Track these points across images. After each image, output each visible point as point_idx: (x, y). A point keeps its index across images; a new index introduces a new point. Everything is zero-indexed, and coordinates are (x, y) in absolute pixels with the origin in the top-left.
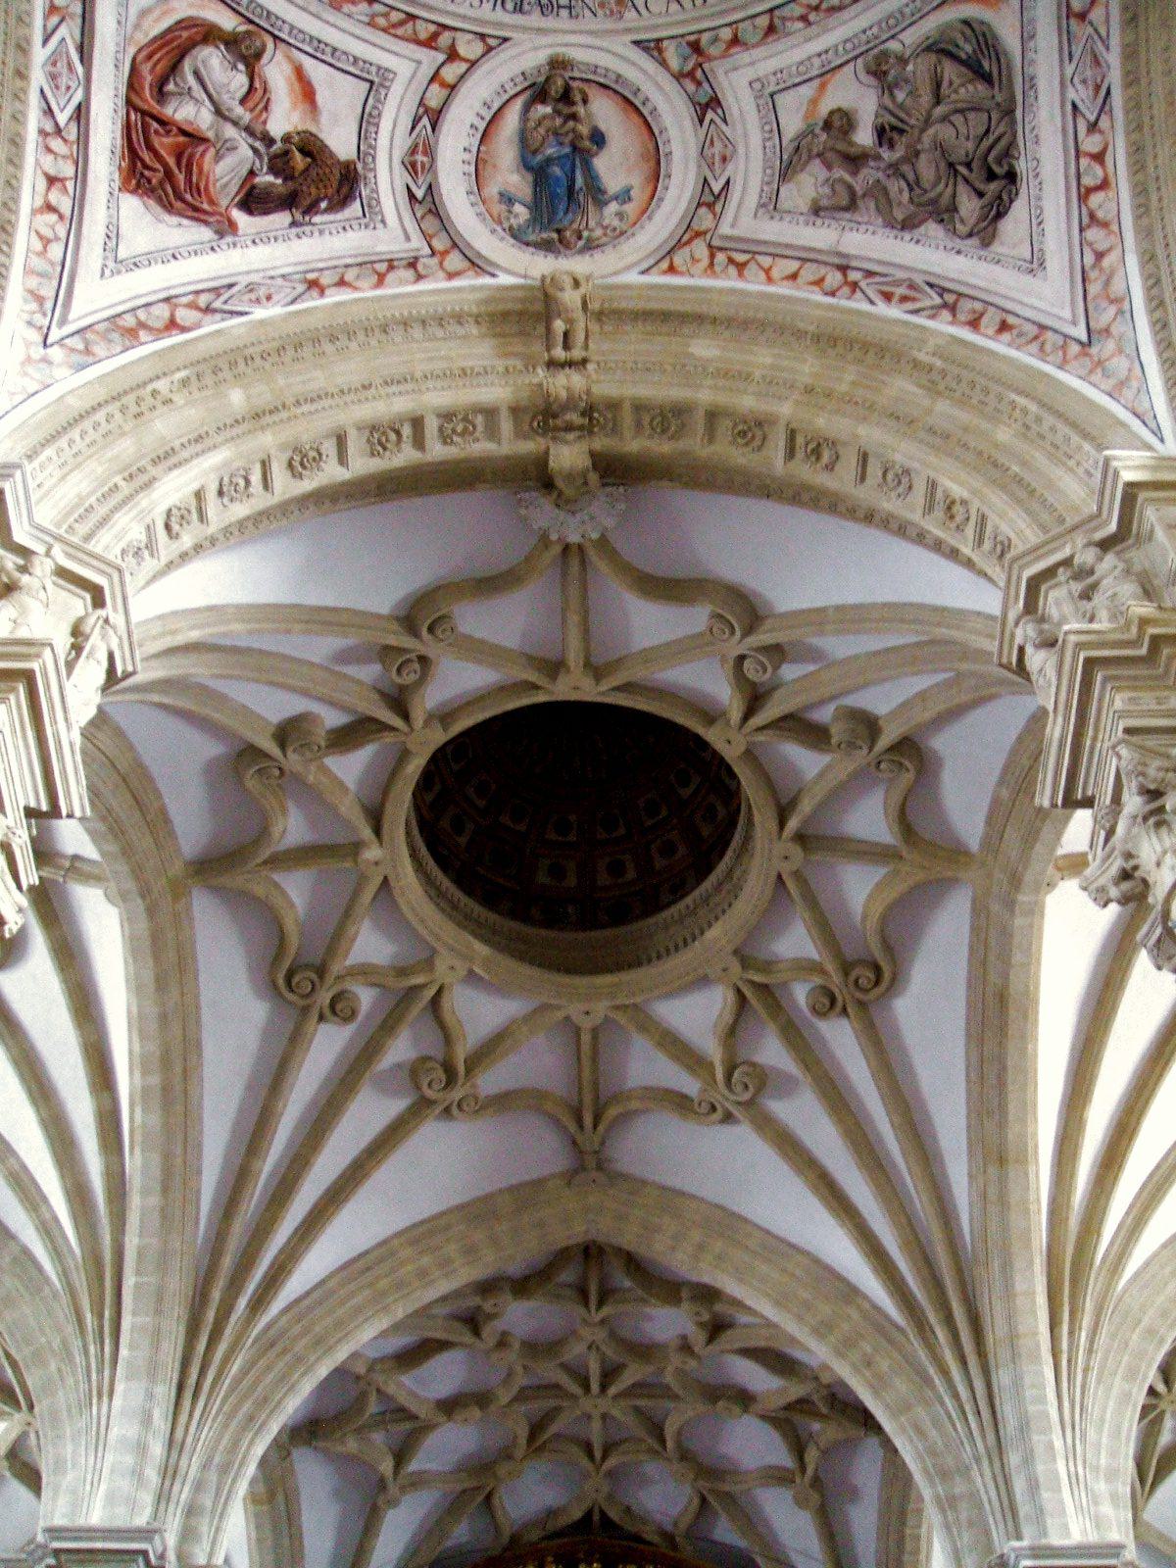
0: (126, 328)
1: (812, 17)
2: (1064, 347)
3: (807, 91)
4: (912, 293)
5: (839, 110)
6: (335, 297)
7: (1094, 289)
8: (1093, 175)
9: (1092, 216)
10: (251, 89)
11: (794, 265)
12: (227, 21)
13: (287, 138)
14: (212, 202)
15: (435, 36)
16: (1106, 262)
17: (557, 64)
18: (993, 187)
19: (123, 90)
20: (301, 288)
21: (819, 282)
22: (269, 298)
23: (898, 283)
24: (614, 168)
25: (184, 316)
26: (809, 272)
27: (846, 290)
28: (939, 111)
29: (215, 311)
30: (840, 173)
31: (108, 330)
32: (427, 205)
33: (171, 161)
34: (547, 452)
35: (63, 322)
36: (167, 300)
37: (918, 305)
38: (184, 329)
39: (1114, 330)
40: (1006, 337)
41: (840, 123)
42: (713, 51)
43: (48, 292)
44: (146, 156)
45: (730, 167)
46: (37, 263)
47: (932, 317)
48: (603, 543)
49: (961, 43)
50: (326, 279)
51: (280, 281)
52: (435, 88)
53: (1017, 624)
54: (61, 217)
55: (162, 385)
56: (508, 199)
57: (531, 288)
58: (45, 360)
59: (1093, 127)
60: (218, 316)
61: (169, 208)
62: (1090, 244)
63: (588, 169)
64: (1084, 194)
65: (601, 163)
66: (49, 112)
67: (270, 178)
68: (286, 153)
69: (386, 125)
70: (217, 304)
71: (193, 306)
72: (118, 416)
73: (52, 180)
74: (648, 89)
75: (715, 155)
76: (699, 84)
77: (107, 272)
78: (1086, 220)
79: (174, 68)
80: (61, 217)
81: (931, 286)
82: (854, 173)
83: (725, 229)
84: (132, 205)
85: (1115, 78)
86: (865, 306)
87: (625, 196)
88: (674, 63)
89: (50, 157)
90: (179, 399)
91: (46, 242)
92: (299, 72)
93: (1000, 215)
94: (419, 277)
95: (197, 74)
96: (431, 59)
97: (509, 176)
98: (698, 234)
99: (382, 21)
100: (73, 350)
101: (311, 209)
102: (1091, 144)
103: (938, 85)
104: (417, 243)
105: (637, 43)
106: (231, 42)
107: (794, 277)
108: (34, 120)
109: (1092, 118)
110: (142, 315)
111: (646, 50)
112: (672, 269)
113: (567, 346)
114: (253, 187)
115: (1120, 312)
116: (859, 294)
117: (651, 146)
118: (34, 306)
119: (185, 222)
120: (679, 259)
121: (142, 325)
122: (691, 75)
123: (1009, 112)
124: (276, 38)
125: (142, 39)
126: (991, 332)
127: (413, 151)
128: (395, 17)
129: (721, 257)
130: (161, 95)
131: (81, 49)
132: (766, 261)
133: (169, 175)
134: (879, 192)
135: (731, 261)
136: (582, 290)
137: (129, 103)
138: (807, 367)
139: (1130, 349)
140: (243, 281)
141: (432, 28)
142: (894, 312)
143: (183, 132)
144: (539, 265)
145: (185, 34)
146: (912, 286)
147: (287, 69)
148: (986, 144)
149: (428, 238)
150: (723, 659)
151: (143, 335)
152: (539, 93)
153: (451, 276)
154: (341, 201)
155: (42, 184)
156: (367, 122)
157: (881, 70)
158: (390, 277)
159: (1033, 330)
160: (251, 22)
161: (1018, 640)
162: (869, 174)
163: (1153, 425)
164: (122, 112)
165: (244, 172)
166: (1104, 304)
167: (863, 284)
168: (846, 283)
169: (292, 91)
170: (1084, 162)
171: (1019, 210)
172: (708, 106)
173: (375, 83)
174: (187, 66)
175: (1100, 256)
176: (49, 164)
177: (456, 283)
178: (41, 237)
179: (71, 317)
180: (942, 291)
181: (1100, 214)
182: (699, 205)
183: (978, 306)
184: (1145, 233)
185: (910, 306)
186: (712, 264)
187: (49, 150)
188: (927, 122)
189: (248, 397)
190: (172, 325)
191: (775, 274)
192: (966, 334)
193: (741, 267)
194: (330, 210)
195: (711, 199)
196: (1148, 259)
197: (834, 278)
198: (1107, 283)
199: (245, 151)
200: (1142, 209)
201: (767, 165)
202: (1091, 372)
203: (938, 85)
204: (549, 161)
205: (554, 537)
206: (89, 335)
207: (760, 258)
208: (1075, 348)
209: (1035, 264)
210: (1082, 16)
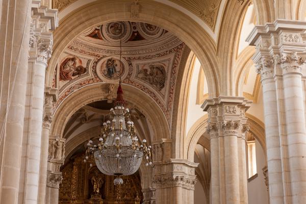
0: (61, 99)
12: (71, 57)
24: (118, 69)
30: (145, 76)
41: (146, 71)
56: (104, 71)
64: (170, 93)
65: (116, 68)
75: (131, 70)
79: (66, 64)
84: (61, 81)
85: (175, 83)
92: (80, 60)
97: (105, 68)
103: (157, 73)
104: (94, 77)
107: (138, 86)
123: (164, 79)
127: (93, 66)
134: (149, 79)
138: (138, 98)
142: (149, 95)
154: (84, 72)
156: (88, 64)
157: (152, 67)
162: (148, 77)
171: (164, 88)
172: (130, 64)
173: (89, 61)
175: (170, 101)
190: (66, 95)
197: (143, 87)
199: (73, 70)
203: (157, 73)
209: (163, 97)
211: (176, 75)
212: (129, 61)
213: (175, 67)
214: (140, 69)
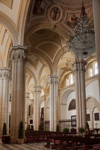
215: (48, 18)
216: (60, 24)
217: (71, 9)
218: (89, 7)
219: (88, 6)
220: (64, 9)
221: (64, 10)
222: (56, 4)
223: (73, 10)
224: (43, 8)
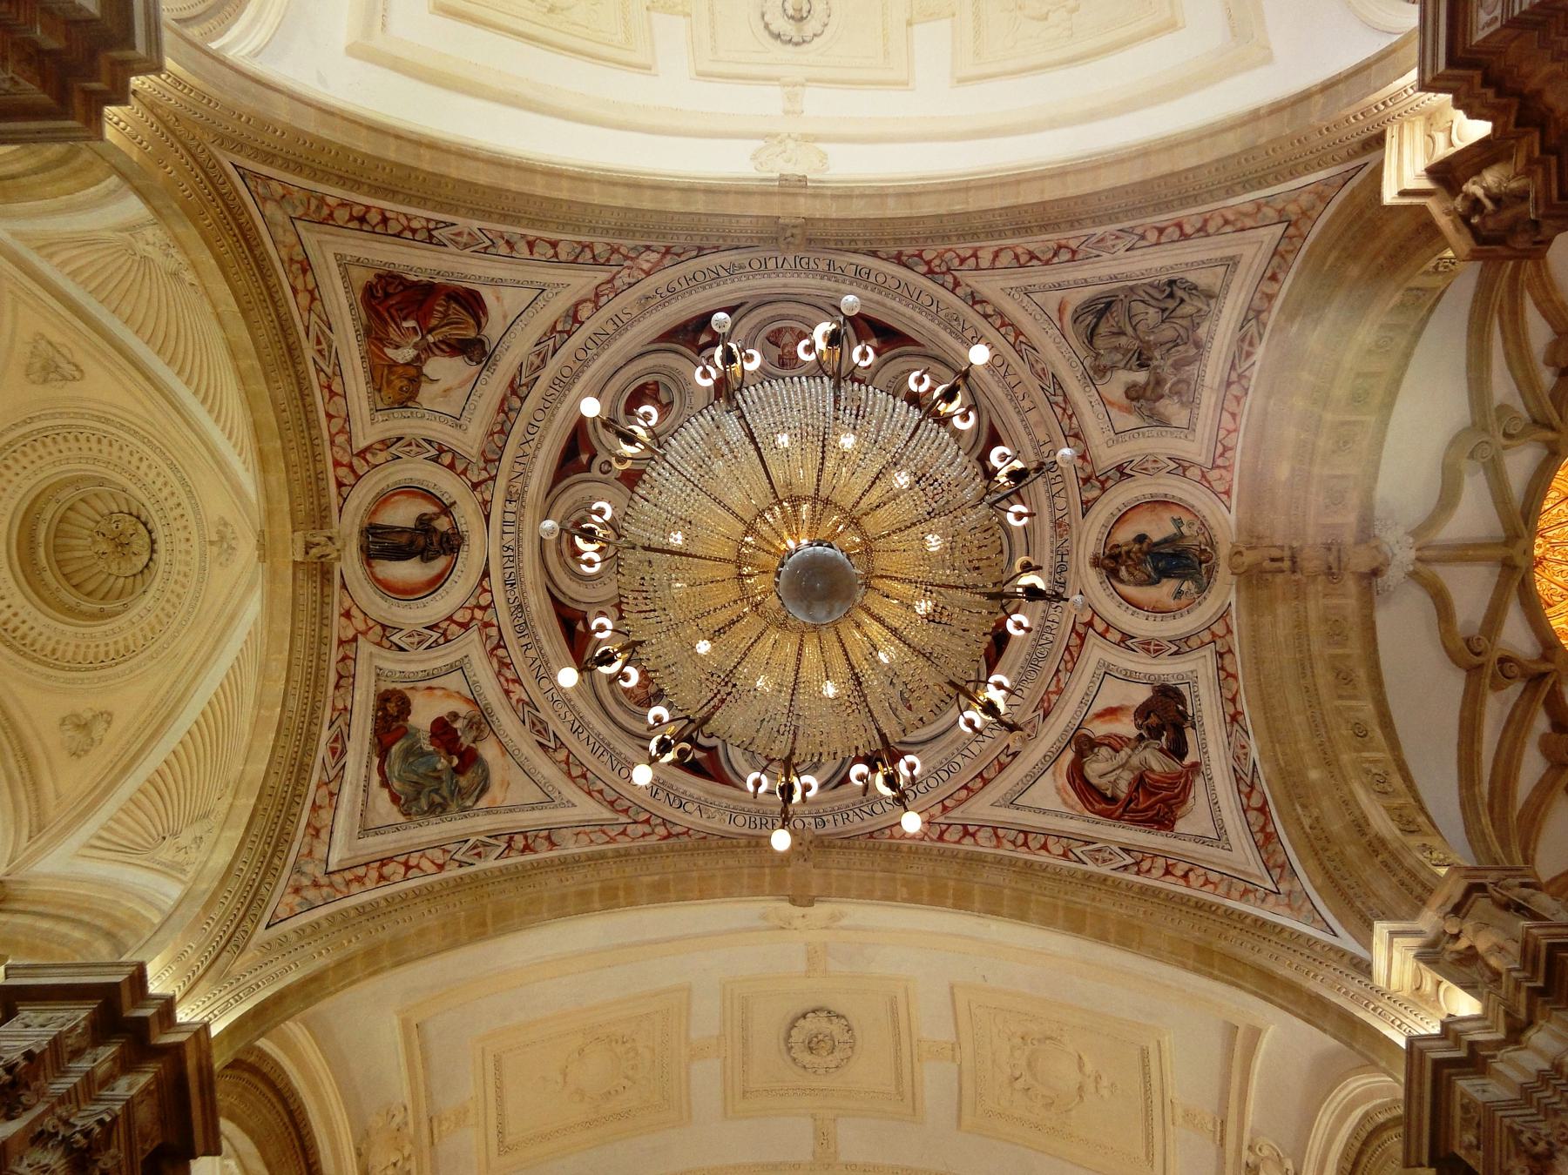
0: (1265, 840)
1: (1070, 412)
2: (1291, 238)
3: (1114, 413)
4: (1248, 337)
5: (1126, 393)
6: (1243, 705)
7: (1249, 222)
8: (1173, 232)
9: (1199, 230)
10: (1109, 745)
11: (1226, 416)
12: (1069, 755)
13: (1139, 727)
14: (1180, 777)
15: (1078, 634)
16: (1231, 217)
17: (1096, 563)
18: (1179, 293)
19: (1110, 821)
20: (1236, 726)
21: (1238, 399)
22: (1243, 747)
23: (1240, 349)
24: (1158, 528)
25: (1256, 801)
26: (1231, 405)
27: (1244, 382)
28: (1129, 330)
29: (1252, 782)
31: (1266, 852)
32: (1181, 647)
33: (1153, 799)
34: (1353, 573)
35: (1262, 879)
36: (1245, 811)
37: (1256, 335)
38: (1266, 802)
39: (1280, 207)
40: (1281, 276)
41: (1134, 394)
42: (1089, 470)
43: (1242, 886)
44: (1151, 813)
45: (1160, 457)
46: (1222, 889)
47: (1265, 325)
48: (1415, 533)
49: (1087, 322)
50: (1232, 711)
51: (1232, 739)
52: (1109, 636)
53: (1515, 249)
54: (1191, 870)
55: (1307, 822)
56: (1179, 594)
57: (1238, 582)
58: (1289, 894)
59: (1143, 237)
60: (1256, 780)
61: (1184, 802)
62: (1219, 229)
63: (1157, 544)
65: (1156, 536)
66: (1126, 868)
67: (1163, 739)
68: (1148, 728)
69: (1131, 666)
70: (1248, 781)
71: (1249, 796)
72: (1327, 854)
73: (1167, 872)
74: (1112, 508)
76: (1108, 478)
77: (1227, 847)
78: (1202, 234)
80: (1191, 870)
81: (1242, 327)
82: (1165, 381)
83: (1200, 460)
84: (1180, 826)
86: (1257, 367)
87: (1178, 522)
88: (1096, 493)
89: (1153, 871)
90: (1316, 812)
91: (1207, 882)
92: (1099, 716)
93: (1196, 288)
94: (1230, 651)
95: (1101, 776)
96: (1092, 638)
97: (1164, 591)
98: (1203, 476)
99: (1070, 665)
100: (1281, 877)
101: (1184, 715)
102: (1152, 236)
104: (1208, 652)
105: (1084, 515)
106: (1080, 755)
107: (1234, 415)
108: (1129, 877)
109: (1136, 238)
110: (1255, 829)
111: (1087, 510)
112: (1228, 493)
113: (1281, 559)
114: (1169, 749)
115: (1267, 204)
116: (1247, 373)
117: (1146, 506)
118: (1251, 896)
119: (1192, 795)
120: (1220, 487)
121: (1262, 829)
122: (1103, 483)
124: (1078, 728)
125: (1080, 806)
126: (1276, 286)
128: (1067, 657)
129: (1219, 462)
130: (1113, 800)
131: (1087, 843)
132: (1222, 433)
133: (1163, 801)
135: (1222, 455)
136: (1243, 549)
137: (1119, 818)
139: (1293, 195)
140: (1231, 761)
141: (1074, 635)
143: (1136, 790)
144: (1223, 575)
145: (1077, 781)
146: (1242, 340)
147: (1097, 723)
148: (1153, 302)
149: (1203, 645)
150: (1505, 448)
151: (1270, 829)
152: (1113, 574)
153: (1229, 631)
155: (1169, 878)
156: (1129, 677)
158: (1230, 669)
159: (1277, 259)
160: (1069, 742)
161: (1528, 246)
163: (1353, 172)
164: (1123, 823)
165: (1160, 754)
166: (1260, 215)
167: (1240, 371)
168: (1239, 382)
169: (1110, 721)
170: (1163, 239)
171: (1192, 277)
172: (1122, 472)
173: (1108, 672)
174: (1095, 781)
175: (1227, 222)
176: (1158, 872)
177: (1235, 629)
178: (1205, 884)
179: (1258, 873)
180: (1246, 320)
181: (1198, 225)
182: (1185, 476)
183: (1258, 295)
184: (1212, 195)
185: (1256, 340)
186: (1224, 467)
187: (1149, 871)
188: (1138, 338)
189: (1315, 767)
190: (1263, 809)
191: (1231, 426)
192: (1278, 303)
193: (1226, 449)
194: (1184, 704)
195: (1181, 467)
196: (1230, 192)
198: (1246, 215)
200: (1196, 199)
201: (1160, 435)
202: (1309, 218)
204: (1155, 569)
205: (1411, 568)
206: (1271, 864)
207: (1220, 437)
208: (1292, 231)
210: (1074, 252)
211: (1071, 237)
212: (1095, 480)
213: (1032, 256)
214: (1133, 421)
215: (358, 478)
216: (350, 634)
217: (509, 674)
218: (612, 803)
219: (611, 796)
220: (478, 614)
221: (473, 618)
222: (487, 518)
223: (507, 692)
224: (426, 392)
